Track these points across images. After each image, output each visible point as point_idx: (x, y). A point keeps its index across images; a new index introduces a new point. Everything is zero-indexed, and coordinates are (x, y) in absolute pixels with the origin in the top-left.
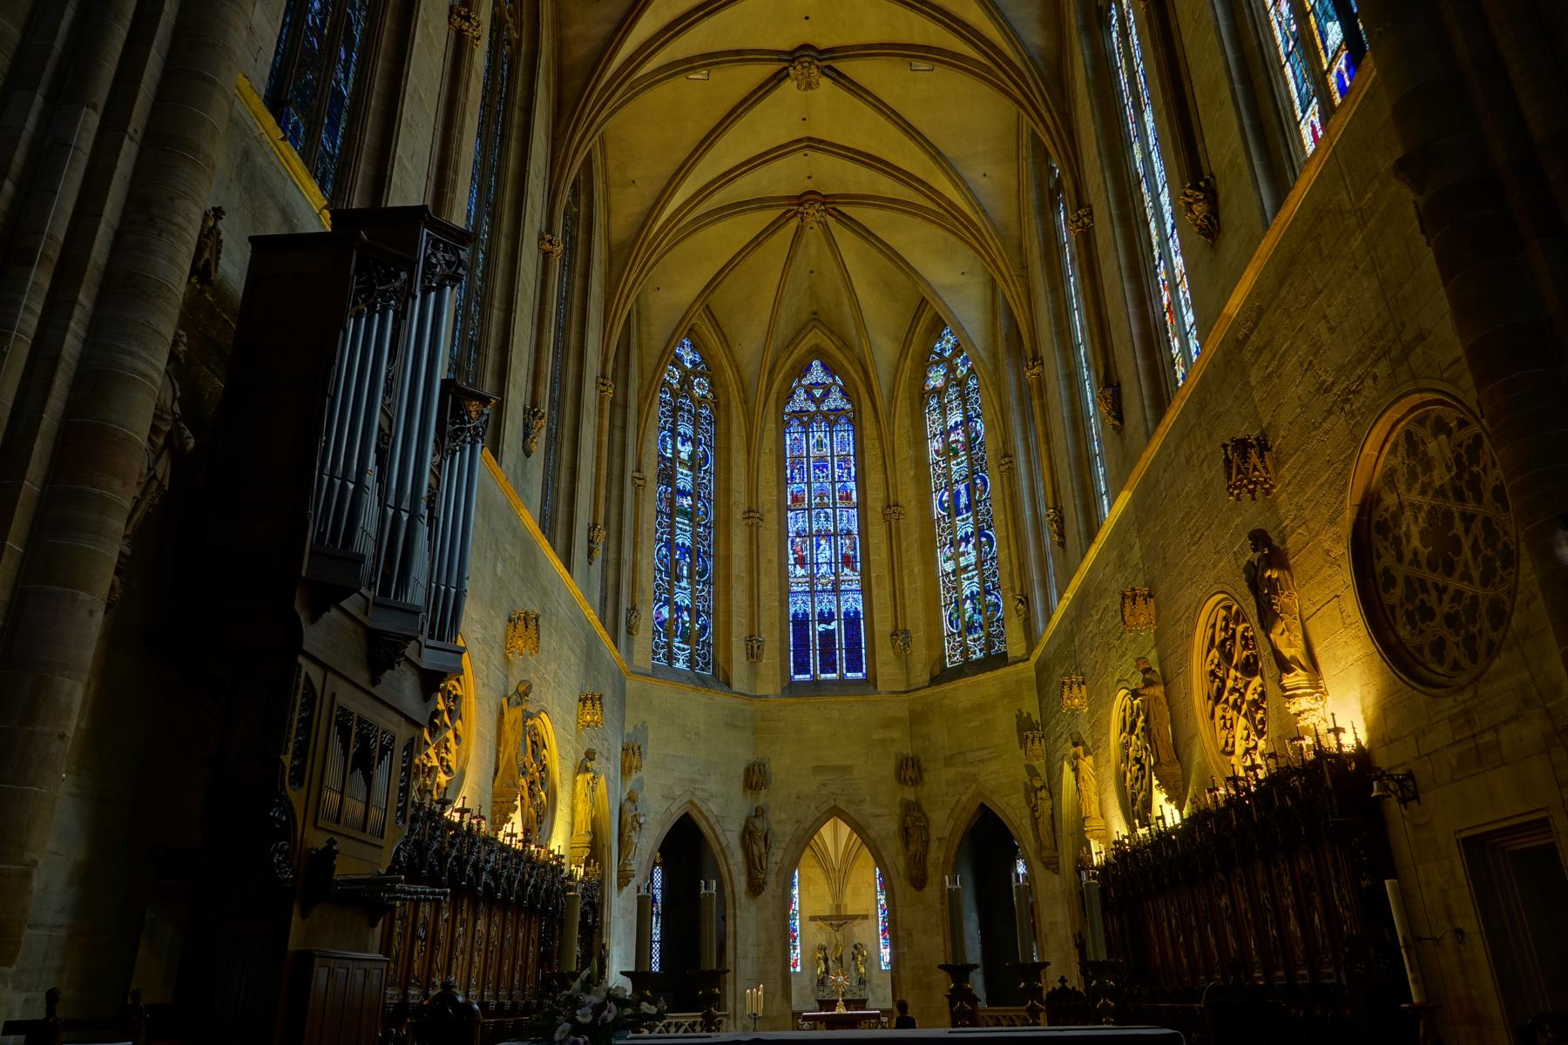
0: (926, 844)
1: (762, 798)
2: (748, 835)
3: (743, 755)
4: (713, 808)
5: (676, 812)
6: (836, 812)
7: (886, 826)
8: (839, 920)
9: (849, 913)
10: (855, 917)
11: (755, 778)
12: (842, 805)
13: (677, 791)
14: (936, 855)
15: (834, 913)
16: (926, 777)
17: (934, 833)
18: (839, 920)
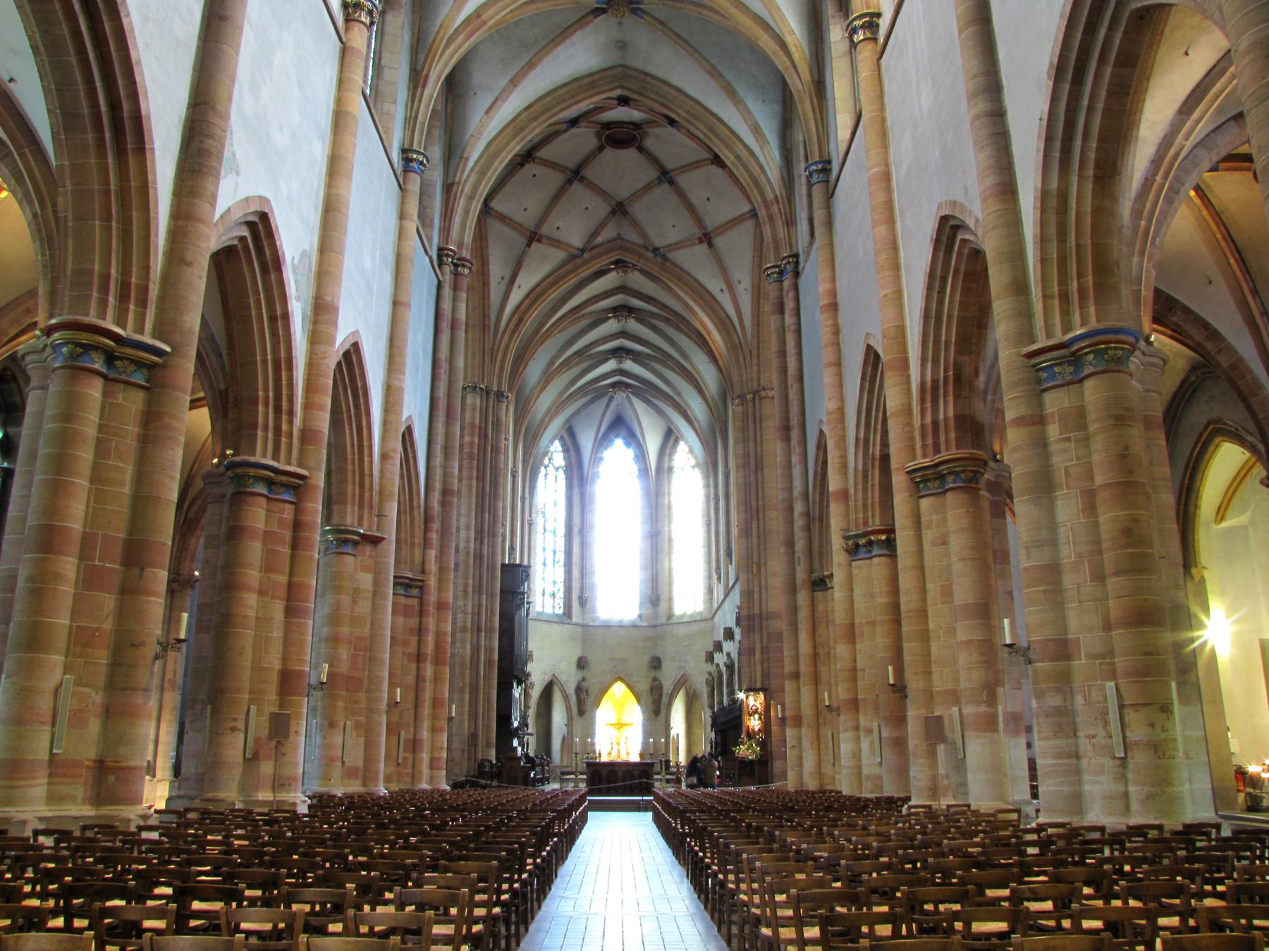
0: (661, 695)
1: (586, 673)
2: (579, 689)
3: (577, 653)
4: (563, 677)
5: (547, 679)
6: (620, 679)
7: (644, 686)
8: (620, 726)
9: (624, 721)
10: (626, 725)
11: (582, 664)
12: (622, 676)
13: (548, 670)
14: (665, 700)
15: (614, 721)
16: (664, 665)
17: (665, 691)
18: (620, 726)
